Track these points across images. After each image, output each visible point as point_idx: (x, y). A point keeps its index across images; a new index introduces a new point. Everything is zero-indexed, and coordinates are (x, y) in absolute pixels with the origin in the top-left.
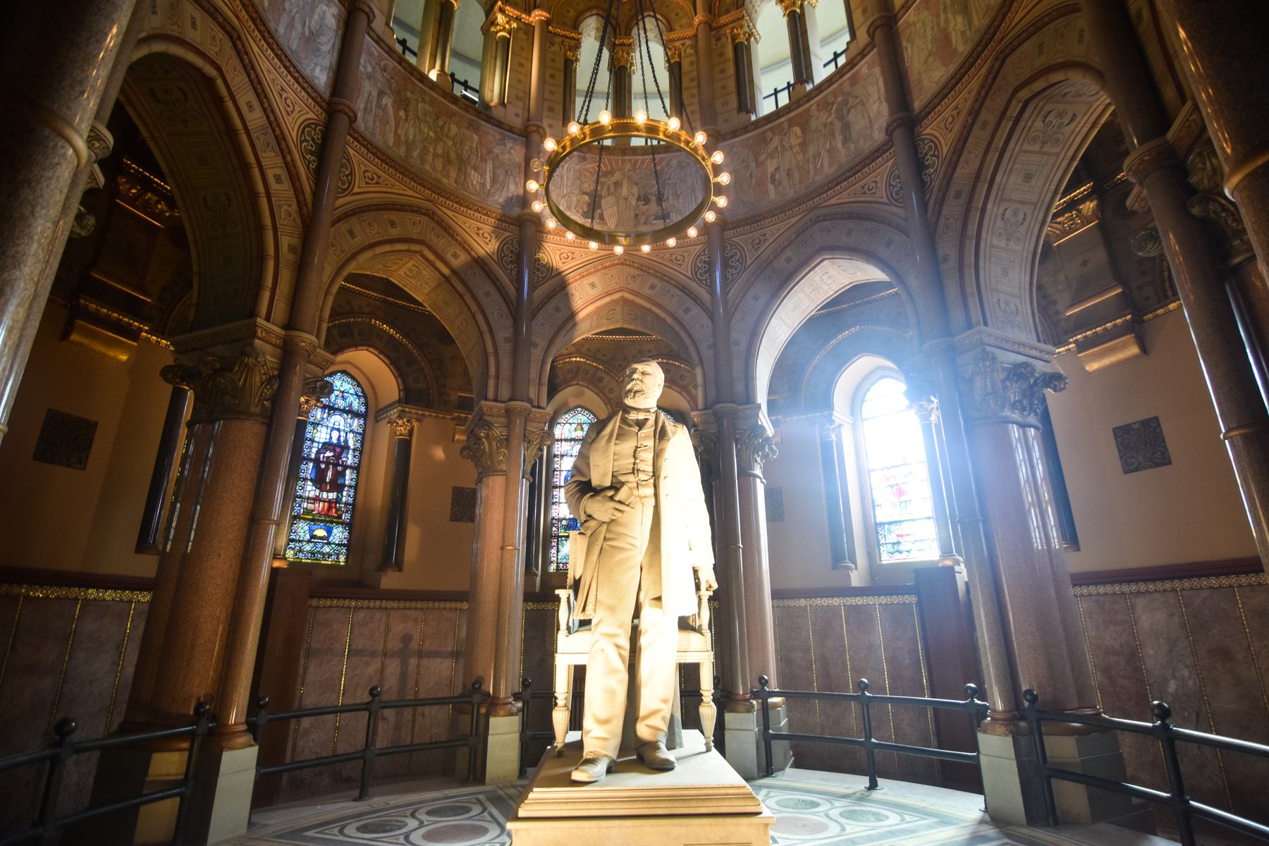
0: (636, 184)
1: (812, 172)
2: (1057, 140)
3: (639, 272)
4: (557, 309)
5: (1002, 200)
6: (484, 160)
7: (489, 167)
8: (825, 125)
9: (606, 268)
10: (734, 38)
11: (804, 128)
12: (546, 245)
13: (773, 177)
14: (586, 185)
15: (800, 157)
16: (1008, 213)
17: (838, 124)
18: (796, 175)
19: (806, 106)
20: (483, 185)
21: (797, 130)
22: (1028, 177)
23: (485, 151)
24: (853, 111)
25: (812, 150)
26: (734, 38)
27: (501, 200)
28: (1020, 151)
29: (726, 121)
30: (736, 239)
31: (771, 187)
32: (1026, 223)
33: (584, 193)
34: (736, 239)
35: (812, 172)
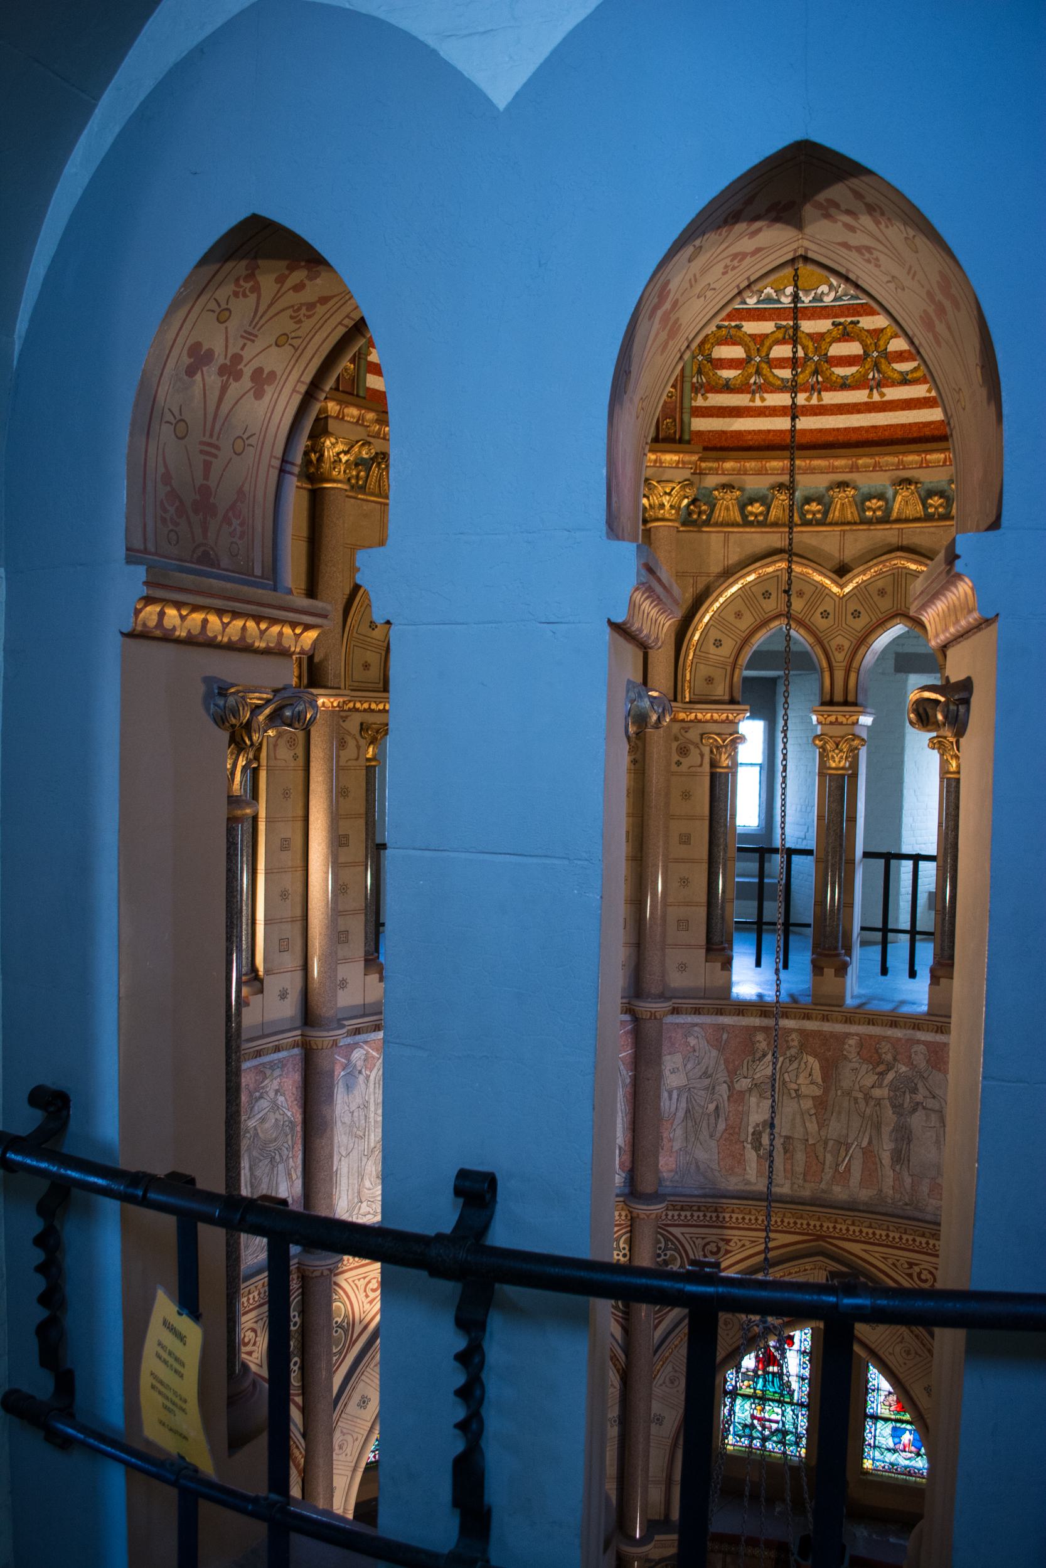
1: (828, 1173)
8: (867, 1097)
10: (713, 764)
11: (830, 1069)
13: (757, 1135)
15: (812, 1127)
17: (889, 1114)
18: (800, 1156)
19: (840, 1028)
21: (813, 1063)
24: (920, 1114)
25: (835, 1128)
26: (713, 764)
29: (682, 967)
30: (676, 1231)
31: (751, 1155)
34: (676, 1231)
35: (828, 1173)
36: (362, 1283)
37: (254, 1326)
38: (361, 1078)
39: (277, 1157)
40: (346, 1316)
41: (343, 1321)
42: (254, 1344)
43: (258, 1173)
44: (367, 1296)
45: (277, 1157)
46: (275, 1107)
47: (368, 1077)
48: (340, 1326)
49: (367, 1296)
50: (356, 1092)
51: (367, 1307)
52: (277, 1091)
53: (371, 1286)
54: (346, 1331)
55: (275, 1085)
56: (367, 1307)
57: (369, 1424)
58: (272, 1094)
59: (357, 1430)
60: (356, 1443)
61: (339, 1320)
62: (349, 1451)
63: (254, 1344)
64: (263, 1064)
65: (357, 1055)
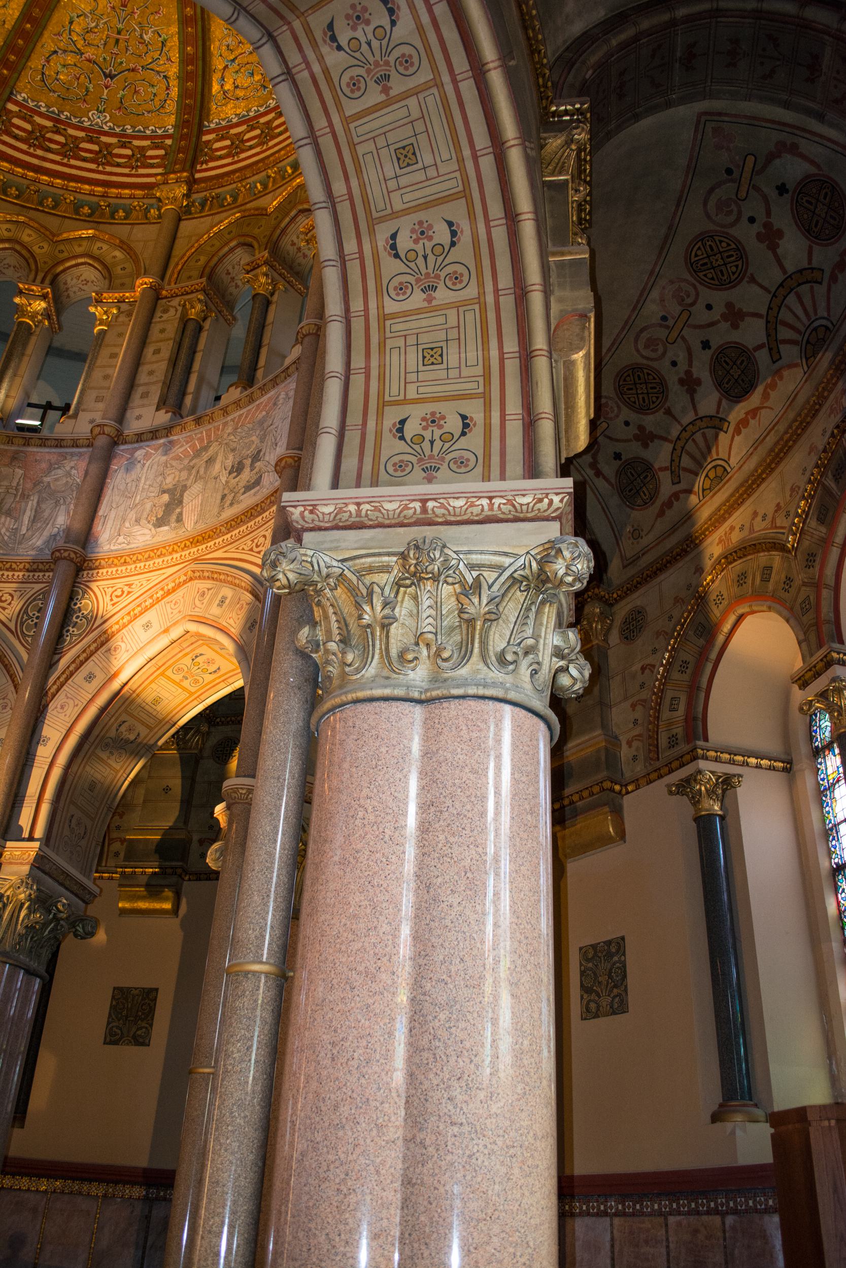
0: (233, 450)
2: (406, 61)
3: (208, 584)
4: (90, 677)
5: (372, 224)
6: (25, 497)
7: (32, 503)
9: (169, 593)
12: (94, 586)
14: (169, 480)
16: (404, 243)
20: (15, 531)
22: (406, 156)
23: (29, 485)
27: (39, 543)
28: (346, 121)
32: (465, 237)
33: (164, 492)
36: (111, 590)
37: (13, 593)
38: (139, 465)
39: (62, 501)
40: (92, 611)
41: (88, 614)
42: (9, 604)
43: (43, 506)
44: (112, 600)
45: (62, 501)
46: (68, 474)
47: (144, 465)
48: (85, 617)
49: (112, 600)
50: (133, 473)
51: (110, 607)
52: (72, 468)
53: (116, 593)
54: (88, 621)
55: (72, 464)
56: (110, 607)
57: (90, 696)
58: (68, 468)
59: (79, 698)
60: (76, 709)
61: (86, 613)
62: (68, 713)
63: (9, 604)
64: (66, 453)
65: (139, 454)
